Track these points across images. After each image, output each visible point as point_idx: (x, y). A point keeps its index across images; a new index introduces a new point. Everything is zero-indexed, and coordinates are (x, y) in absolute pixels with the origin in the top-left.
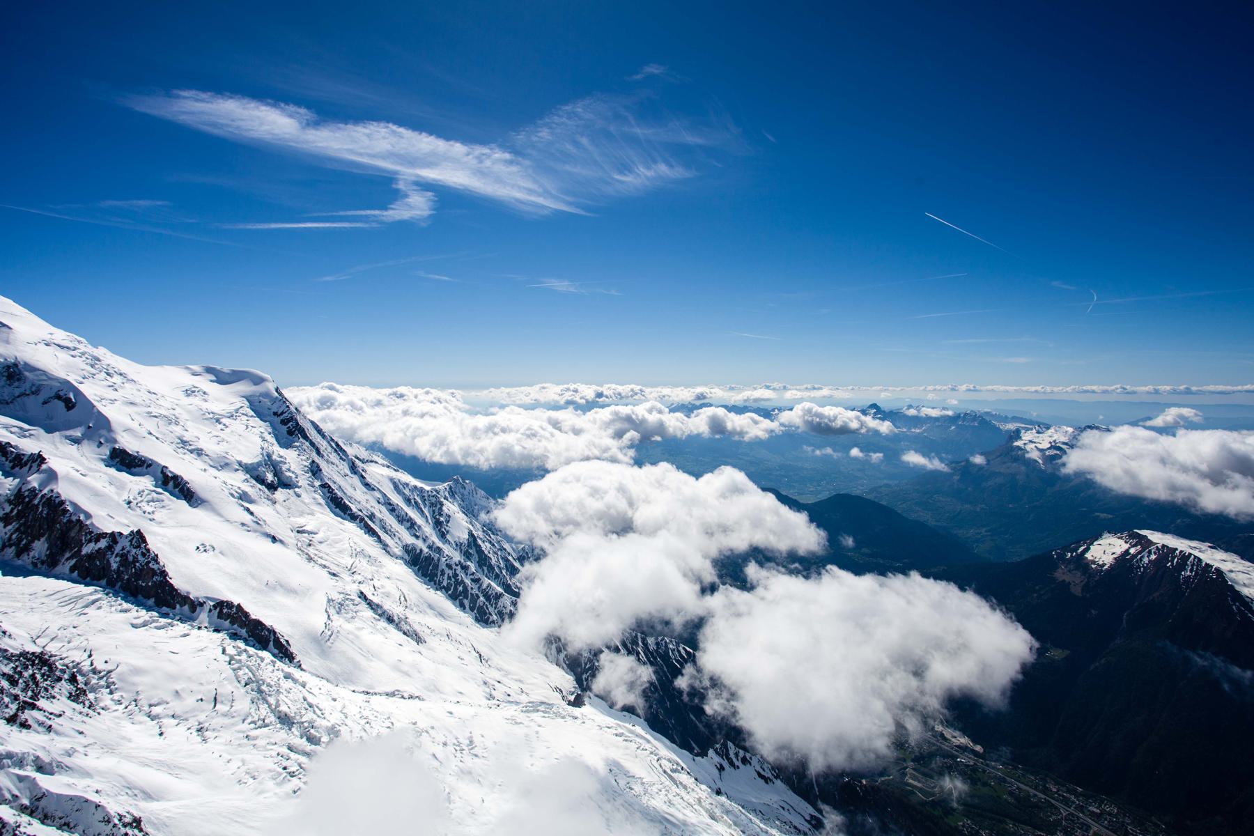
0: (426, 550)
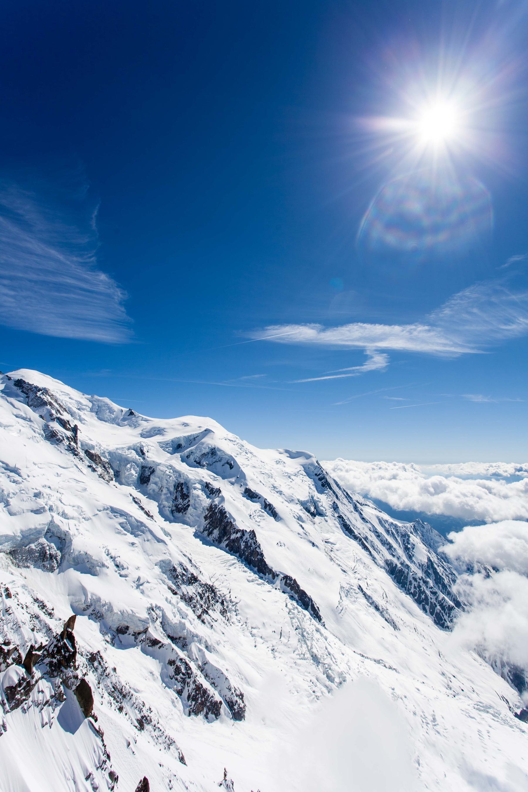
0: (399, 565)
